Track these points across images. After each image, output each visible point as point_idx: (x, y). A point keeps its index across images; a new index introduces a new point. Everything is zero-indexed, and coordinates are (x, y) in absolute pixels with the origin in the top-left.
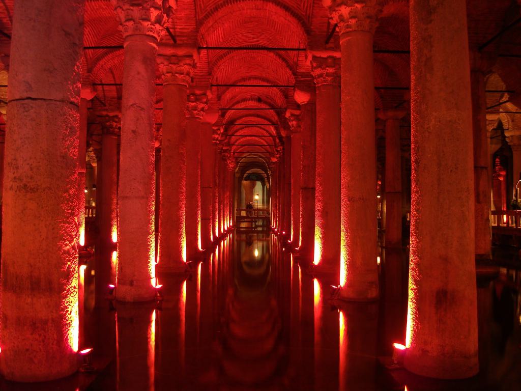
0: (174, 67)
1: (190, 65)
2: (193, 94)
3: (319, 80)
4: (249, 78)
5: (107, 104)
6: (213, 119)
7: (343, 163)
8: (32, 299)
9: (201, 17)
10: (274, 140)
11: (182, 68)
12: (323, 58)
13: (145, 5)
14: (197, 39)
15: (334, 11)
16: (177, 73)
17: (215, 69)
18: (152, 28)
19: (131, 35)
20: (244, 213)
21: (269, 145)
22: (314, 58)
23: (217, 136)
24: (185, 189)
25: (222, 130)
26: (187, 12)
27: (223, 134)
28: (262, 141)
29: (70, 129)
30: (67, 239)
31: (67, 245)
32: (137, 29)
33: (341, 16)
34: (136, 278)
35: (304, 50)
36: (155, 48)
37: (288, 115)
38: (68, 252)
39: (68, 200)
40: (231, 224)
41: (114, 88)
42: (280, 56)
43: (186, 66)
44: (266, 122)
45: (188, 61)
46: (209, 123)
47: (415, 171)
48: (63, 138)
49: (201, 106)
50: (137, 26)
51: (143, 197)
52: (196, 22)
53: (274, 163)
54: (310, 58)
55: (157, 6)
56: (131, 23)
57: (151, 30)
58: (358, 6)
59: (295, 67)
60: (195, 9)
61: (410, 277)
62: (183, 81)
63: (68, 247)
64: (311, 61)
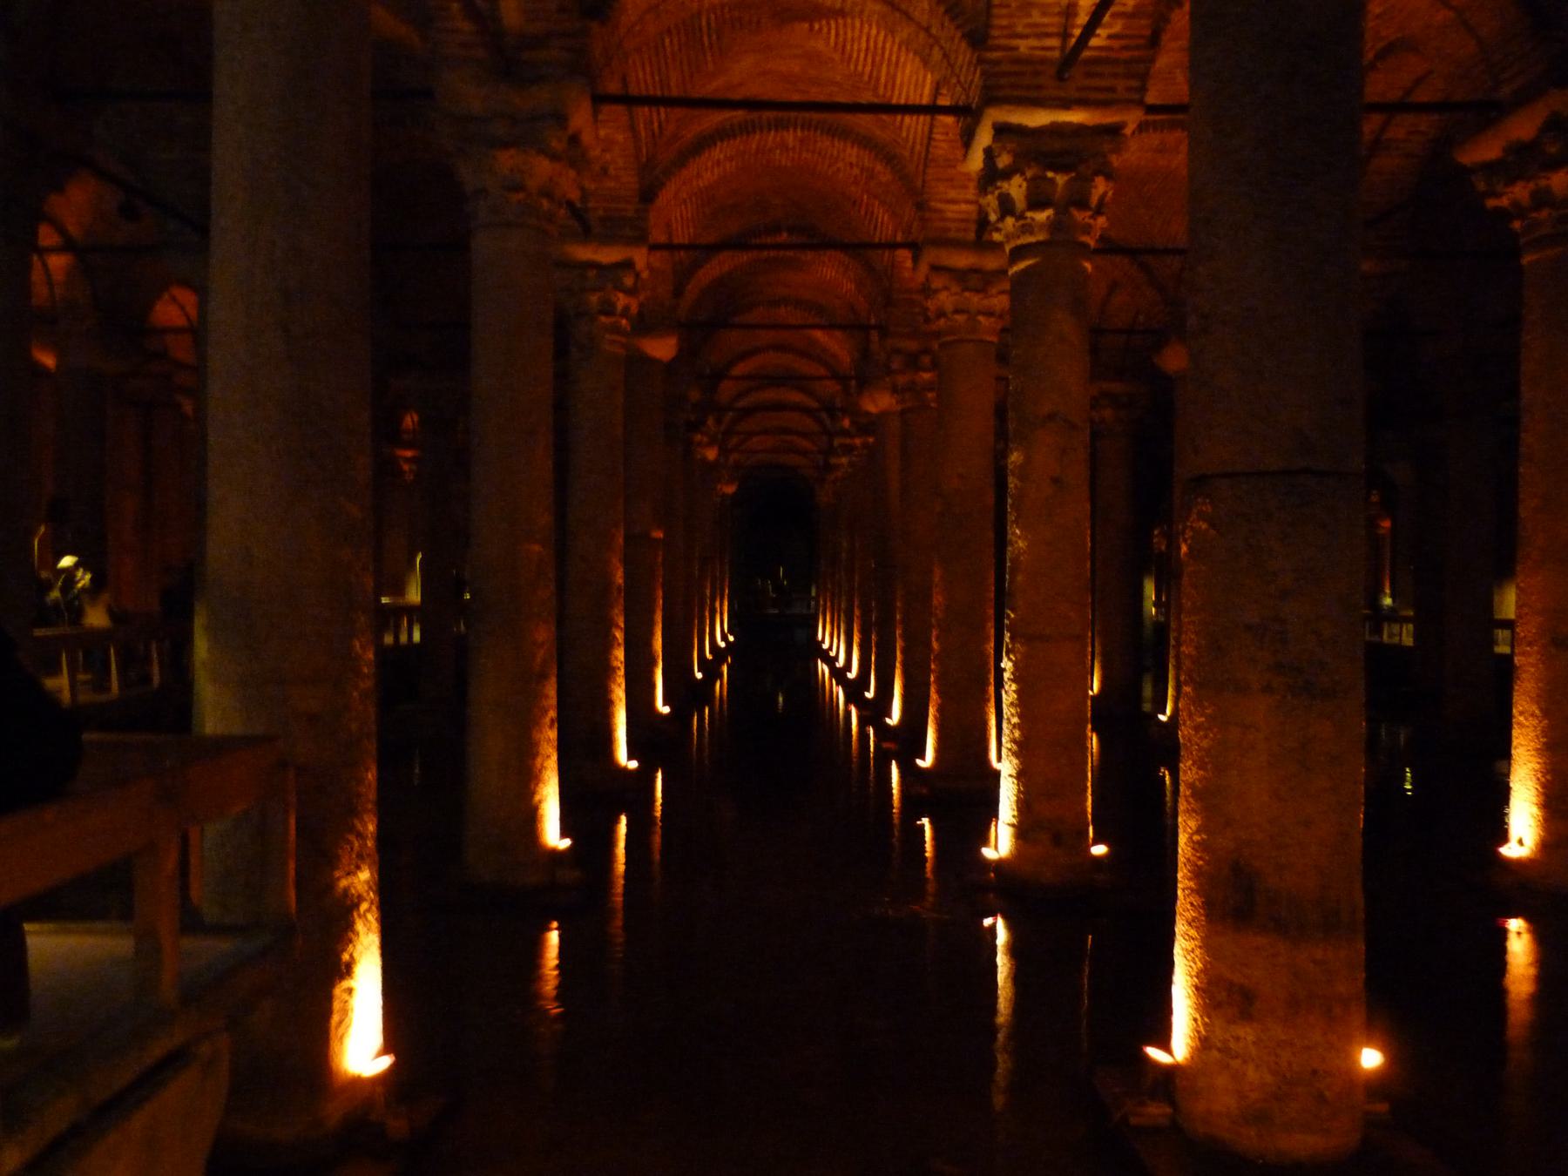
0: (975, 300)
11: (995, 301)
16: (980, 313)
18: (1090, 226)
32: (1054, 226)
56: (1042, 216)
57: (1087, 230)
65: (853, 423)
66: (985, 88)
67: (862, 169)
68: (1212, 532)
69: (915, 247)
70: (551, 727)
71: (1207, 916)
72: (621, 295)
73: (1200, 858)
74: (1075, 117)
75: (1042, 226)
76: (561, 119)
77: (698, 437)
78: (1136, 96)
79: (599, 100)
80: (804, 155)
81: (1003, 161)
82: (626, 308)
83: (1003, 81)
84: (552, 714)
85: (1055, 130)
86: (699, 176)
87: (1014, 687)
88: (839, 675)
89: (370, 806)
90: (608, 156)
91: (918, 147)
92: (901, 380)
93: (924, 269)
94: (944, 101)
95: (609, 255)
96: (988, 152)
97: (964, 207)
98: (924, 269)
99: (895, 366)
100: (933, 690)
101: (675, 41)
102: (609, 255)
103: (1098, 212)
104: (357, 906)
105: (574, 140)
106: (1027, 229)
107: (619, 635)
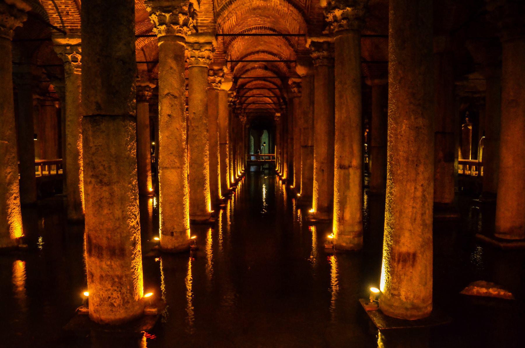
0: (197, 53)
1: (210, 50)
2: (212, 69)
3: (317, 61)
4: (258, 52)
5: (139, 76)
6: (226, 86)
7: (336, 138)
8: (111, 262)
9: (217, 10)
10: (279, 100)
11: (203, 53)
12: (320, 43)
13: (174, 11)
14: (215, 29)
15: (329, 12)
16: (199, 57)
17: (229, 48)
18: (180, 30)
19: (163, 36)
20: (253, 158)
21: (274, 103)
22: (313, 43)
23: (231, 99)
24: (208, 152)
25: (235, 94)
26: (207, 6)
27: (235, 97)
28: (268, 99)
29: (131, 136)
30: (133, 218)
31: (132, 222)
32: (168, 31)
33: (335, 17)
34: (175, 230)
35: (303, 35)
36: (183, 46)
37: (290, 82)
38: (133, 227)
39: (132, 190)
40: (243, 169)
41: (145, 64)
43: (206, 52)
44: (272, 86)
45: (208, 47)
46: (223, 90)
47: (390, 163)
48: (126, 144)
49: (218, 79)
50: (168, 29)
51: (179, 168)
52: (214, 15)
53: (278, 117)
54: (309, 41)
55: (185, 12)
56: (163, 27)
58: (349, 9)
60: (213, 3)
61: (384, 241)
62: (205, 63)
63: (133, 223)
64: (310, 46)
70: (15, 198)
75: (163, 31)
90: (68, 8)
106: (160, 32)
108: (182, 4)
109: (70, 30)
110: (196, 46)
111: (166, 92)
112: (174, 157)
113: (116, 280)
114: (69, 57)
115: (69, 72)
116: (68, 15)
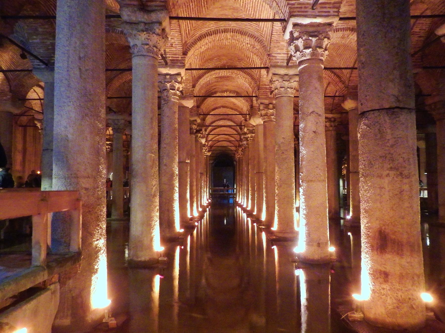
0: (286, 84)
11: (292, 84)
16: (288, 88)
42: (335, 74)
43: (295, 83)
56: (308, 51)
59: (347, 82)
65: (248, 130)
66: (290, 12)
67: (251, 45)
68: (368, 128)
69: (267, 68)
71: (372, 250)
72: (177, 84)
73: (368, 231)
74: (319, 20)
76: (160, 23)
77: (199, 135)
78: (337, 14)
79: (171, 18)
80: (233, 41)
81: (296, 34)
82: (179, 88)
83: (295, 10)
84: (158, 207)
85: (311, 25)
86: (201, 47)
87: (304, 197)
88: (245, 210)
89: (104, 219)
90: (173, 40)
91: (268, 37)
92: (263, 112)
93: (270, 75)
94: (277, 17)
95: (173, 71)
96: (291, 33)
97: (282, 55)
98: (270, 75)
99: (261, 108)
100: (276, 205)
101: (194, 4)
102: (173, 71)
103: (326, 50)
104: (99, 251)
105: (163, 30)
107: (177, 189)
108: (328, 29)
109: (171, 60)
110: (286, 78)
111: (311, 111)
112: (320, 171)
113: (416, 278)
114: (168, 85)
115: (166, 99)
116: (172, 46)
